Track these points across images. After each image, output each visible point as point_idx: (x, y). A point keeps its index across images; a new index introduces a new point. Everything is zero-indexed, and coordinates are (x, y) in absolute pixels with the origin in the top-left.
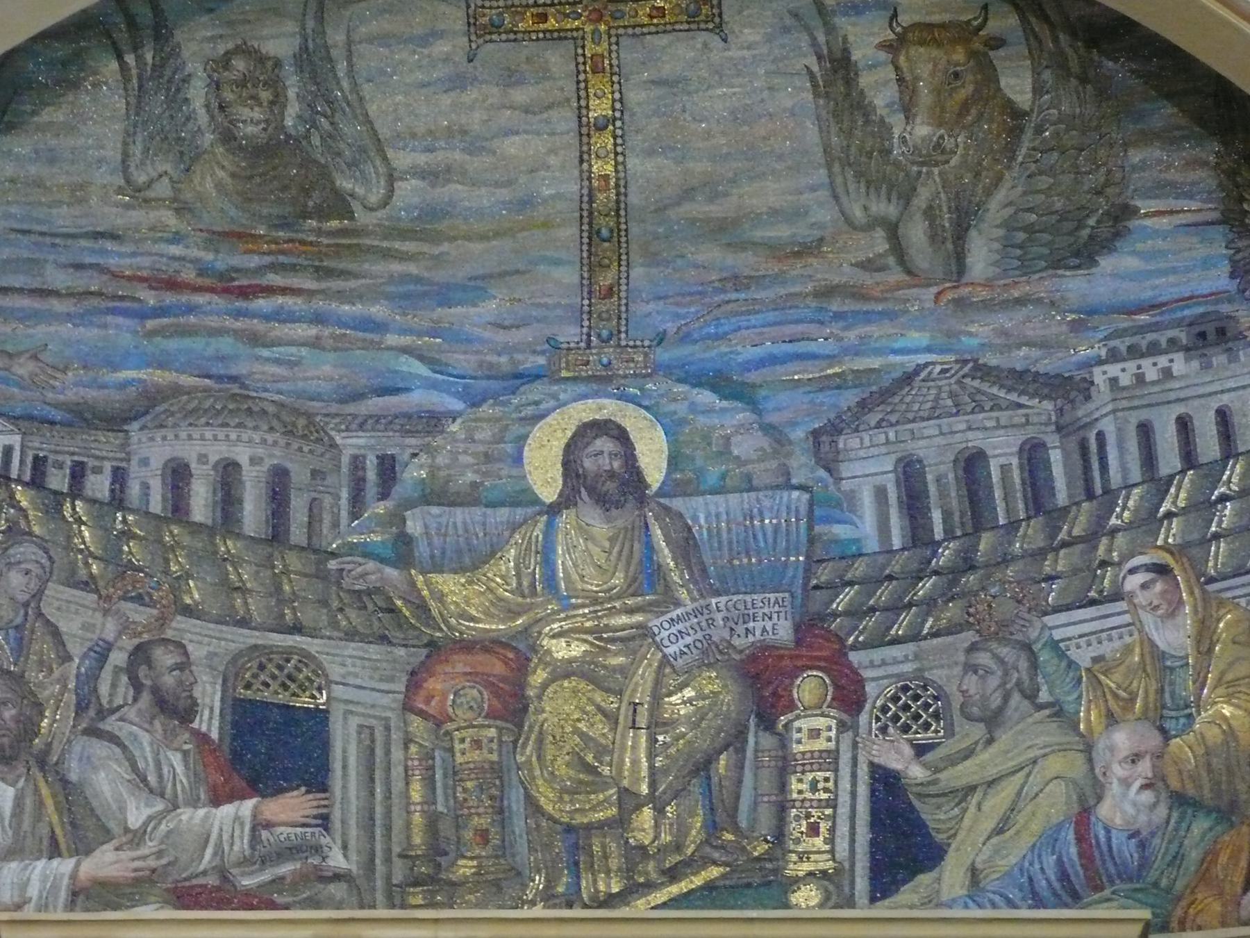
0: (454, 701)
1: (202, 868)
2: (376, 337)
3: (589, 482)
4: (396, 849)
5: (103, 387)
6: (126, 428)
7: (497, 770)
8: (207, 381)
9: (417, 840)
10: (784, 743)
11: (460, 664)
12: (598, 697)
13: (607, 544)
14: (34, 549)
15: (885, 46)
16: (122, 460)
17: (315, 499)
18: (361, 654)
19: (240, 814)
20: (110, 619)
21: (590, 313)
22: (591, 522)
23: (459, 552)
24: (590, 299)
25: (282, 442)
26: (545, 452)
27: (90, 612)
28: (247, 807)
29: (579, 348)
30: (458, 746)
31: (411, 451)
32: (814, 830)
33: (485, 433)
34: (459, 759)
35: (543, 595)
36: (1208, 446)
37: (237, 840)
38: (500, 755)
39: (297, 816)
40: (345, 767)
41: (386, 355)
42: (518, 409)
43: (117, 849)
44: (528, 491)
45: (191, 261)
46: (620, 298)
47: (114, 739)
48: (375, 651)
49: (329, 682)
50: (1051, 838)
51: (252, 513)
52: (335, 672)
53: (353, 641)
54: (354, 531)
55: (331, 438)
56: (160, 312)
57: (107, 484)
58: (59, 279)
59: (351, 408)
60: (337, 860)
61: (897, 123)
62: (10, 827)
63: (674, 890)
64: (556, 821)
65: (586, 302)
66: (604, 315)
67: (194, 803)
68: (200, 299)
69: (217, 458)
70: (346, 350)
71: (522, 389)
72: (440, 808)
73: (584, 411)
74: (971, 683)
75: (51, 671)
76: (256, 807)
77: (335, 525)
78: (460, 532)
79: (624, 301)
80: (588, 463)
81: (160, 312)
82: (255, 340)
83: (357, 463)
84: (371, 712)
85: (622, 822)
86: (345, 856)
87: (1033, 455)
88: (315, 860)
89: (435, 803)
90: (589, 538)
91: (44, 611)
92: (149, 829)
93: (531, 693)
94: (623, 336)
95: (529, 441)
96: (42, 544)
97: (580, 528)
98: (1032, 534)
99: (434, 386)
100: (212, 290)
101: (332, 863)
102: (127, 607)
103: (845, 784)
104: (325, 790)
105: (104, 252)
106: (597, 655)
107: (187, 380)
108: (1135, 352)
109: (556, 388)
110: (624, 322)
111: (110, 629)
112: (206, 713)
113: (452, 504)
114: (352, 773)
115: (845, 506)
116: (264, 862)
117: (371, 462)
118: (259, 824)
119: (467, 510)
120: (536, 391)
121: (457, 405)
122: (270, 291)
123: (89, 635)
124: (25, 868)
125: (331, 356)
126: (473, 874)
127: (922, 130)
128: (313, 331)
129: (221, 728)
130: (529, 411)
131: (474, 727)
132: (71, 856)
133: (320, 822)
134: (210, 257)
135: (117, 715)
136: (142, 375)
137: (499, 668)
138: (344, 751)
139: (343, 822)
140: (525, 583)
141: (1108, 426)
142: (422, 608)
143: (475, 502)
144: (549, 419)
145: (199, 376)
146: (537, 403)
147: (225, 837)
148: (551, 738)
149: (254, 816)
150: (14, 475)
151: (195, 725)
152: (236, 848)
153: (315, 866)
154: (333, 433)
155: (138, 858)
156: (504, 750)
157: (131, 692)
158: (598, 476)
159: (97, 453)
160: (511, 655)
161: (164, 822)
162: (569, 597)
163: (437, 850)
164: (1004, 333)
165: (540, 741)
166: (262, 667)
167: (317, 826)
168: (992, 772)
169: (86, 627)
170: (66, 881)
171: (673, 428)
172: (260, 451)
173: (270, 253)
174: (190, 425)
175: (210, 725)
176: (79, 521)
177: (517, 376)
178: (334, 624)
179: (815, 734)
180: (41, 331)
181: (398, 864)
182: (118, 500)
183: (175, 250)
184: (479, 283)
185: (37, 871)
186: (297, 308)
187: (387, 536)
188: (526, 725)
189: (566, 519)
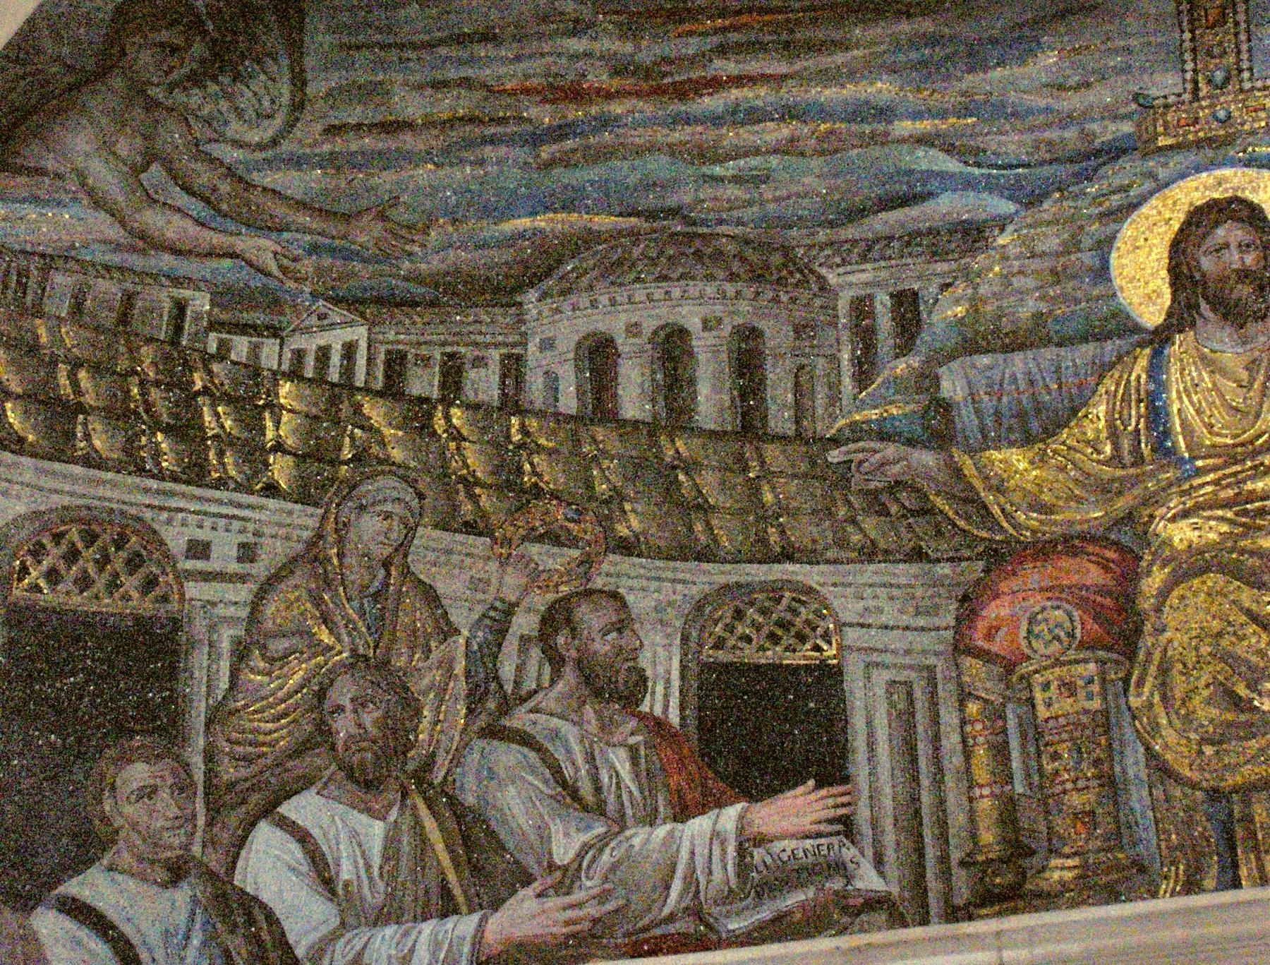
0: (1029, 632)
1: (666, 911)
2: (881, 127)
3: (1210, 292)
4: (956, 855)
5: (483, 246)
6: (519, 300)
7: (1104, 722)
8: (633, 220)
9: (987, 837)
11: (1033, 576)
12: (1246, 596)
13: (1244, 375)
14: (392, 482)
16: (514, 345)
17: (802, 367)
18: (886, 579)
19: (719, 827)
20: (510, 570)
21: (1194, 50)
22: (1216, 346)
23: (1021, 415)
24: (1192, 31)
25: (749, 292)
26: (1141, 254)
27: (480, 564)
28: (729, 816)
29: (1183, 103)
30: (1039, 696)
31: (940, 280)
33: (1051, 241)
34: (1042, 712)
35: (1153, 462)
37: (717, 867)
38: (1105, 699)
39: (806, 822)
40: (871, 746)
41: (894, 150)
42: (1096, 200)
43: (539, 896)
45: (602, 58)
46: (1237, 24)
47: (525, 740)
48: (904, 572)
49: (841, 626)
52: (848, 609)
53: (870, 562)
54: (862, 406)
55: (820, 278)
56: (561, 131)
57: (495, 379)
58: (412, 106)
59: (849, 232)
60: (869, 880)
62: (381, 875)
64: (1194, 786)
65: (1187, 35)
66: (1216, 51)
67: (651, 819)
68: (617, 108)
69: (656, 323)
70: (836, 151)
71: (1101, 171)
72: (1019, 788)
73: (1197, 189)
75: (428, 651)
76: (741, 817)
77: (834, 399)
78: (1022, 385)
79: (1243, 26)
80: (1207, 263)
81: (561, 131)
82: (704, 154)
83: (862, 307)
84: (908, 660)
86: (881, 874)
88: (837, 884)
89: (1009, 779)
91: (413, 569)
92: (585, 864)
93: (1146, 605)
94: (1246, 75)
95: (1118, 244)
96: (401, 472)
97: (1203, 358)
99: (969, 184)
100: (638, 94)
101: (859, 884)
102: (534, 549)
104: (846, 779)
105: (472, 61)
106: (1244, 536)
107: (604, 222)
109: (1151, 164)
110: (1245, 56)
111: (512, 583)
112: (660, 688)
113: (1008, 349)
114: (883, 749)
117: (883, 301)
118: (748, 841)
119: (1030, 354)
120: (1124, 172)
121: (1008, 207)
122: (715, 84)
123: (480, 596)
124: (406, 934)
125: (816, 163)
126: (1078, 877)
128: (785, 132)
129: (682, 708)
130: (1116, 200)
131: (1062, 664)
132: (471, 911)
133: (839, 827)
134: (629, 48)
135: (531, 704)
136: (541, 222)
137: (1095, 576)
138: (869, 723)
139: (875, 824)
140: (1126, 444)
142: (970, 500)
143: (1047, 342)
144: (1145, 209)
145: (621, 215)
146: (1124, 189)
147: (700, 862)
148: (1180, 666)
149: (740, 830)
150: (360, 379)
151: (645, 708)
152: (718, 875)
153: (836, 893)
154: (823, 271)
155: (572, 906)
156: (1111, 690)
157: (547, 669)
158: (1223, 279)
159: (480, 339)
160: (1110, 554)
161: (608, 850)
162: (1194, 458)
165: (1164, 670)
166: (739, 615)
167: (838, 833)
169: (478, 584)
170: (466, 949)
172: (718, 309)
173: (716, 31)
174: (612, 283)
175: (666, 707)
176: (458, 437)
177: (1097, 153)
178: (842, 543)
180: (385, 180)
181: (961, 878)
182: (511, 404)
183: (577, 45)
184: (1026, 32)
185: (424, 938)
186: (759, 103)
187: (908, 409)
188: (1141, 656)
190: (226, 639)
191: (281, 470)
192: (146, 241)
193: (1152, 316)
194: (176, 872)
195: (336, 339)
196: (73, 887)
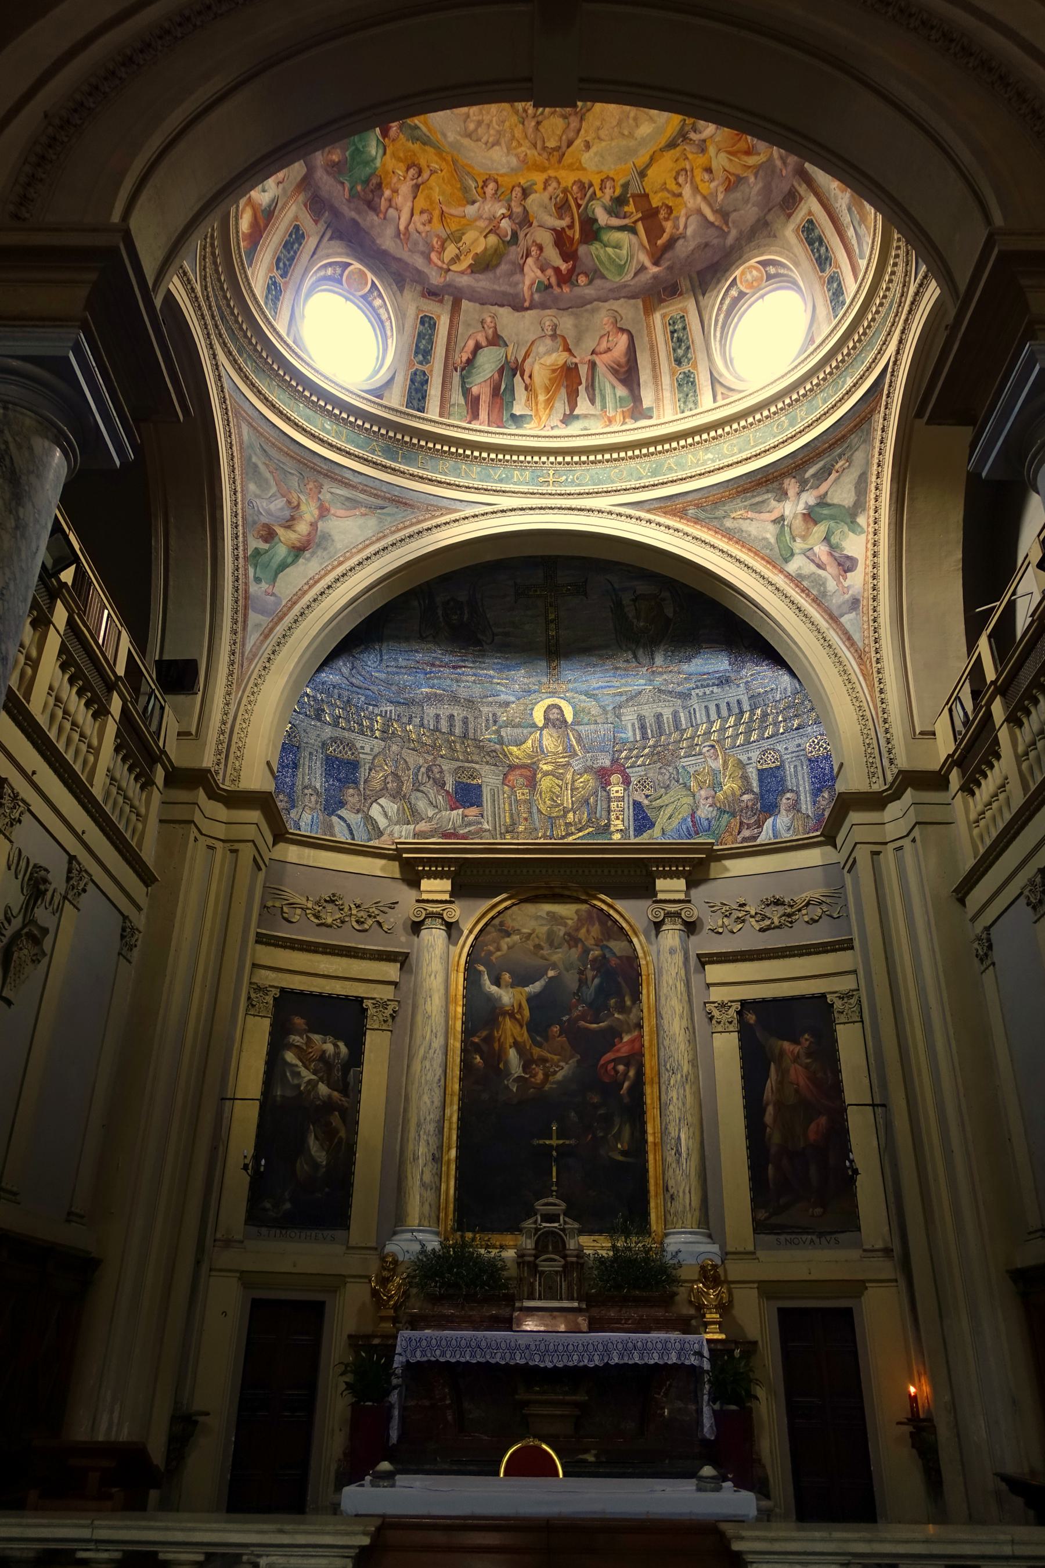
7: (529, 802)
10: (608, 793)
11: (518, 772)
15: (633, 600)
32: (618, 818)
36: (724, 712)
44: (534, 723)
50: (684, 820)
51: (458, 731)
58: (403, 663)
60: (486, 826)
61: (635, 621)
63: (581, 834)
74: (660, 777)
80: (551, 716)
81: (431, 672)
85: (565, 816)
87: (675, 714)
90: (551, 736)
98: (675, 736)
103: (626, 806)
108: (702, 686)
111: (421, 761)
115: (624, 729)
116: (466, 826)
118: (464, 816)
120: (533, 696)
122: (461, 667)
127: (642, 624)
136: (427, 690)
137: (529, 773)
141: (696, 706)
142: (505, 755)
163: (513, 824)
164: (665, 680)
168: (667, 802)
171: (573, 708)
179: (617, 792)
189: (544, 732)
190: (367, 766)
191: (377, 733)
192: (352, 684)
193: (540, 725)
194: (358, 811)
195: (389, 708)
196: (339, 812)
